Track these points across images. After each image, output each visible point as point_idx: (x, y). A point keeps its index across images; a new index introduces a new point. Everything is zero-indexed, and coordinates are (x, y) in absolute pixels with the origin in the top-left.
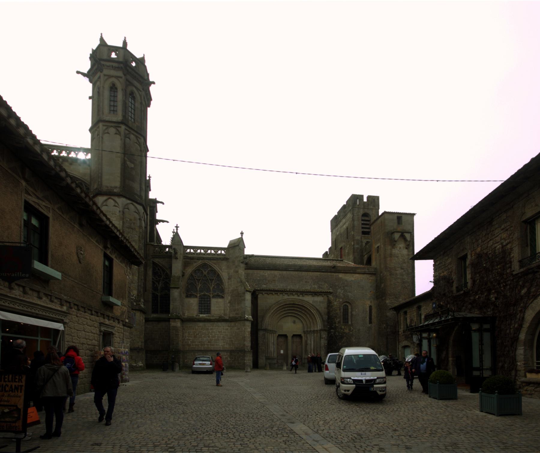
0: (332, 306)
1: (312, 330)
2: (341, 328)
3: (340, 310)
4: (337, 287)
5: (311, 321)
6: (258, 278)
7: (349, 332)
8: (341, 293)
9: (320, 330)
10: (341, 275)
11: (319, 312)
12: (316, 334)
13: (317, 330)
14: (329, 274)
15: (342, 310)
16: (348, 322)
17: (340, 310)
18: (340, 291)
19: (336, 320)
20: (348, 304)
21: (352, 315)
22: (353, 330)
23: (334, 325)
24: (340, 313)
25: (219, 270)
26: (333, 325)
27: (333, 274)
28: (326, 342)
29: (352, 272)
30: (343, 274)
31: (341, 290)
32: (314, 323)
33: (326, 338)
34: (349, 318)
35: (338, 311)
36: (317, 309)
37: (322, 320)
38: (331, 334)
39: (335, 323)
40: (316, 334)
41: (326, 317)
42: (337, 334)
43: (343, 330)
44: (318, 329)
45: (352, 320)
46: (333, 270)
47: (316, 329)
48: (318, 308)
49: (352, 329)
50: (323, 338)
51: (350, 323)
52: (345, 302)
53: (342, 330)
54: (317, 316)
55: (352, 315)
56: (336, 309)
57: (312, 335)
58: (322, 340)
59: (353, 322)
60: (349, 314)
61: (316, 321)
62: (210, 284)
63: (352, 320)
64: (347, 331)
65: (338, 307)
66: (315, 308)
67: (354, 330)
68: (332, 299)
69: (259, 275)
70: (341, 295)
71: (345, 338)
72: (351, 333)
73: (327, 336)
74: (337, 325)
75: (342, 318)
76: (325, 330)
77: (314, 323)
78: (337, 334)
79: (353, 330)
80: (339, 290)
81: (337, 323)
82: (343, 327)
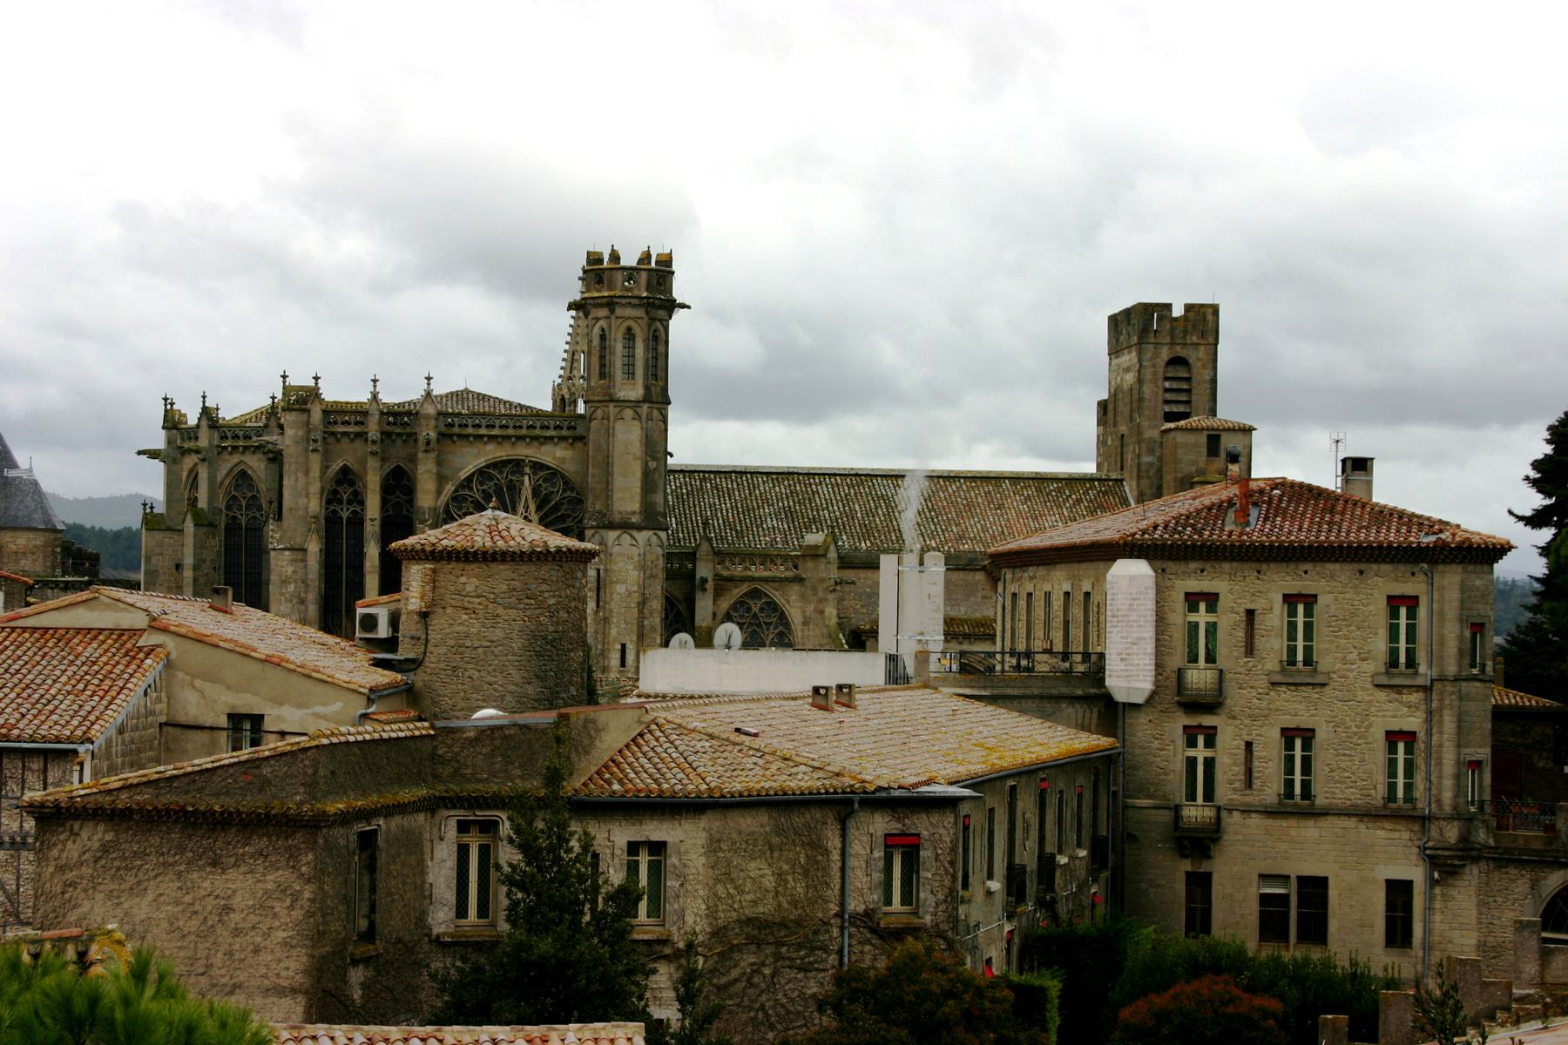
6: (868, 590)
25: (784, 601)
62: (767, 632)
69: (869, 582)
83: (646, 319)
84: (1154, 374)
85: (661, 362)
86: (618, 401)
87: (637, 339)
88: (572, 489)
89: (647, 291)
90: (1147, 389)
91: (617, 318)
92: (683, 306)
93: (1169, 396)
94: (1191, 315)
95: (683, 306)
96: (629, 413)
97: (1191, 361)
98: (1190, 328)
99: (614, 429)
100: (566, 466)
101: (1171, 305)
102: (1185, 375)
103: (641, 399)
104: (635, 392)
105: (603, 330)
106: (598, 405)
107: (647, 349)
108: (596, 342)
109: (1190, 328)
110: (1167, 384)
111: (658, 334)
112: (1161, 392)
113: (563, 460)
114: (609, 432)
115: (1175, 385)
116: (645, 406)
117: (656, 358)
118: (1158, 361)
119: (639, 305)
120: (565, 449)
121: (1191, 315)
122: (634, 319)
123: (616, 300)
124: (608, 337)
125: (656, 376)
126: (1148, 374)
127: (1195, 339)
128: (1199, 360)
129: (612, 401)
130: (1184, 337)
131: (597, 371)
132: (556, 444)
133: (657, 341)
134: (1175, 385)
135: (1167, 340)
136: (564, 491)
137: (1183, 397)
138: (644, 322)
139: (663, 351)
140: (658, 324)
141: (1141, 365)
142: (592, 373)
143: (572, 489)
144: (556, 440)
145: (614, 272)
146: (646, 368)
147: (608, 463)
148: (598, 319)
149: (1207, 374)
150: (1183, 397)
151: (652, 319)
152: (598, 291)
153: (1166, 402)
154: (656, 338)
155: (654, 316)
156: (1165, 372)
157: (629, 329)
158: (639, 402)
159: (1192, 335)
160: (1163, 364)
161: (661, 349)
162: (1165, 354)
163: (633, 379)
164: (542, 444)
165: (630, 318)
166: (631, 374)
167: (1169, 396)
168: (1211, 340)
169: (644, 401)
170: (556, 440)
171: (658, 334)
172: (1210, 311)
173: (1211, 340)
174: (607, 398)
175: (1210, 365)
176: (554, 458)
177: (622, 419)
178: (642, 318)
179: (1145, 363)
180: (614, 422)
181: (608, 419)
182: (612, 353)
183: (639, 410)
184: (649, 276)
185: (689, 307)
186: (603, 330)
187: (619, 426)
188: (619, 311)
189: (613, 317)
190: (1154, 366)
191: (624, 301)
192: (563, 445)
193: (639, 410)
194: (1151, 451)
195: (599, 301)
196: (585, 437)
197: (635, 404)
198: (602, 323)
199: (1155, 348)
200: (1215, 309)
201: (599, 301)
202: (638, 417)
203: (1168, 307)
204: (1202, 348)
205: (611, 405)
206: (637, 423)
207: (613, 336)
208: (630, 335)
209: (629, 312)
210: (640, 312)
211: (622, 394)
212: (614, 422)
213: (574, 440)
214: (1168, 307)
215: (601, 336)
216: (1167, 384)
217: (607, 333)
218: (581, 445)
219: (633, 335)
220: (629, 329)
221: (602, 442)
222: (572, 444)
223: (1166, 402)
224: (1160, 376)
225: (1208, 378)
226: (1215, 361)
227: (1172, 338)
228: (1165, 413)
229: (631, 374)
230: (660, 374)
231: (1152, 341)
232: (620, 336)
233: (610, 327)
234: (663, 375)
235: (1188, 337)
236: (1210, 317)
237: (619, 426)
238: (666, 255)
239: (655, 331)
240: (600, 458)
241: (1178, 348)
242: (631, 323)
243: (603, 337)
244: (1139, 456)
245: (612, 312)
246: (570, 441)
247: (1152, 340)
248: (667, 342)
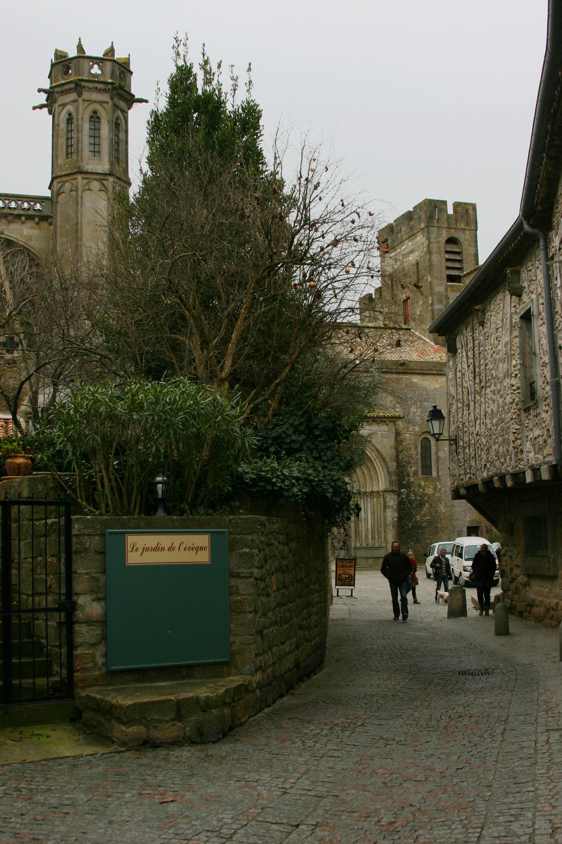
0: (401, 441)
1: (368, 490)
2: (420, 486)
3: (416, 448)
4: (410, 403)
5: (366, 472)
7: (434, 494)
8: (418, 414)
9: (385, 491)
10: (415, 379)
11: (382, 456)
12: (375, 499)
13: (378, 492)
14: (395, 376)
15: (419, 449)
16: (431, 474)
17: (416, 448)
18: (415, 410)
19: (409, 468)
20: (429, 437)
21: (438, 458)
22: (440, 489)
23: (406, 479)
24: (417, 454)
26: (404, 480)
27: (401, 376)
28: (396, 515)
29: (434, 372)
30: (420, 377)
31: (417, 408)
32: (371, 477)
33: (395, 507)
34: (433, 464)
35: (413, 452)
36: (377, 450)
37: (386, 472)
38: (402, 498)
39: (408, 475)
40: (375, 499)
41: (393, 466)
42: (412, 497)
43: (424, 490)
44: (381, 489)
45: (438, 468)
46: (401, 369)
47: (375, 489)
48: (379, 447)
49: (439, 486)
50: (389, 508)
51: (434, 474)
52: (424, 433)
53: (421, 490)
54: (378, 464)
55: (438, 458)
56: (408, 446)
57: (369, 500)
58: (388, 510)
59: (440, 474)
60: (433, 457)
61: (377, 473)
63: (438, 468)
64: (430, 491)
65: (413, 442)
66: (373, 448)
67: (443, 489)
68: (402, 426)
70: (417, 418)
71: (427, 505)
72: (438, 494)
73: (396, 503)
74: (412, 479)
75: (420, 464)
76: (393, 491)
77: (371, 477)
78: (412, 497)
79: (440, 489)
80: (413, 409)
81: (411, 474)
82: (423, 483)
83: (111, 103)
84: (439, 248)
85: (122, 147)
86: (86, 173)
87: (102, 121)
88: (37, 265)
89: (112, 79)
90: (435, 258)
91: (84, 100)
92: (141, 101)
93: (450, 264)
94: (459, 209)
95: (141, 101)
96: (96, 185)
97: (462, 240)
98: (459, 218)
99: (82, 197)
100: (32, 243)
101: (446, 202)
102: (458, 250)
103: (108, 172)
104: (103, 166)
105: (70, 114)
106: (65, 179)
107: (110, 130)
108: (63, 125)
109: (459, 218)
110: (447, 256)
111: (119, 121)
112: (444, 261)
113: (30, 238)
114: (77, 202)
115: (452, 257)
116: (111, 179)
117: (118, 144)
118: (440, 239)
119: (105, 91)
120: (32, 228)
121: (459, 209)
122: (101, 103)
123: (83, 84)
124: (75, 119)
125: (118, 159)
126: (434, 247)
127: (463, 226)
128: (466, 240)
129: (81, 172)
130: (456, 224)
131: (64, 151)
132: (23, 223)
133: (118, 130)
134: (452, 257)
135: (445, 225)
136: (30, 267)
137: (457, 265)
138: (109, 106)
139: (124, 138)
140: (119, 113)
141: (429, 242)
142: (59, 153)
143: (37, 265)
144: (23, 218)
145: (81, 60)
146: (110, 154)
147: (77, 229)
148: (64, 105)
149: (472, 250)
150: (457, 265)
151: (116, 106)
152: (64, 80)
153: (448, 268)
154: (117, 125)
155: (117, 104)
156: (445, 247)
157: (95, 112)
158: (105, 174)
159: (461, 223)
160: (444, 241)
161: (122, 136)
162: (445, 235)
163: (100, 156)
164: (9, 222)
165: (95, 102)
166: (96, 152)
167: (450, 264)
168: (473, 227)
169: (111, 174)
170: (23, 218)
171: (119, 121)
172: (471, 207)
173: (473, 227)
174: (75, 170)
175: (473, 244)
176: (22, 235)
177: (90, 190)
178: (107, 103)
179: (432, 240)
180: (82, 192)
181: (77, 191)
182: (79, 130)
183: (105, 183)
184: (113, 66)
185: (146, 101)
186: (70, 114)
187: (87, 196)
188: (86, 95)
189: (80, 100)
190: (438, 242)
191: (91, 85)
192: (30, 223)
193: (105, 183)
194: (440, 302)
195: (66, 87)
196: (51, 217)
197: (102, 177)
198: (70, 108)
199: (438, 230)
200: (474, 207)
201: (66, 87)
202: (105, 189)
203: (444, 203)
204: (468, 232)
205: (79, 177)
206: (103, 194)
207: (80, 116)
208: (95, 118)
209: (95, 96)
210: (105, 97)
211: (89, 167)
212: (82, 192)
213: (40, 220)
214: (444, 203)
215: (68, 120)
216: (447, 256)
217: (74, 115)
218: (45, 224)
219: (98, 118)
220: (95, 112)
221: (71, 212)
222: (38, 224)
223: (448, 268)
224: (443, 249)
225: (472, 253)
226: (476, 242)
227: (448, 224)
228: (448, 276)
229: (96, 152)
230: (122, 157)
231: (436, 225)
232: (87, 118)
233: (77, 109)
234: (124, 159)
235: (459, 224)
236: (471, 212)
237: (87, 196)
238: (124, 59)
239: (117, 119)
240: (68, 227)
241: (453, 231)
242: (97, 107)
243: (70, 119)
244: (432, 305)
245: (80, 95)
246: (37, 220)
247: (436, 225)
248: (127, 131)
